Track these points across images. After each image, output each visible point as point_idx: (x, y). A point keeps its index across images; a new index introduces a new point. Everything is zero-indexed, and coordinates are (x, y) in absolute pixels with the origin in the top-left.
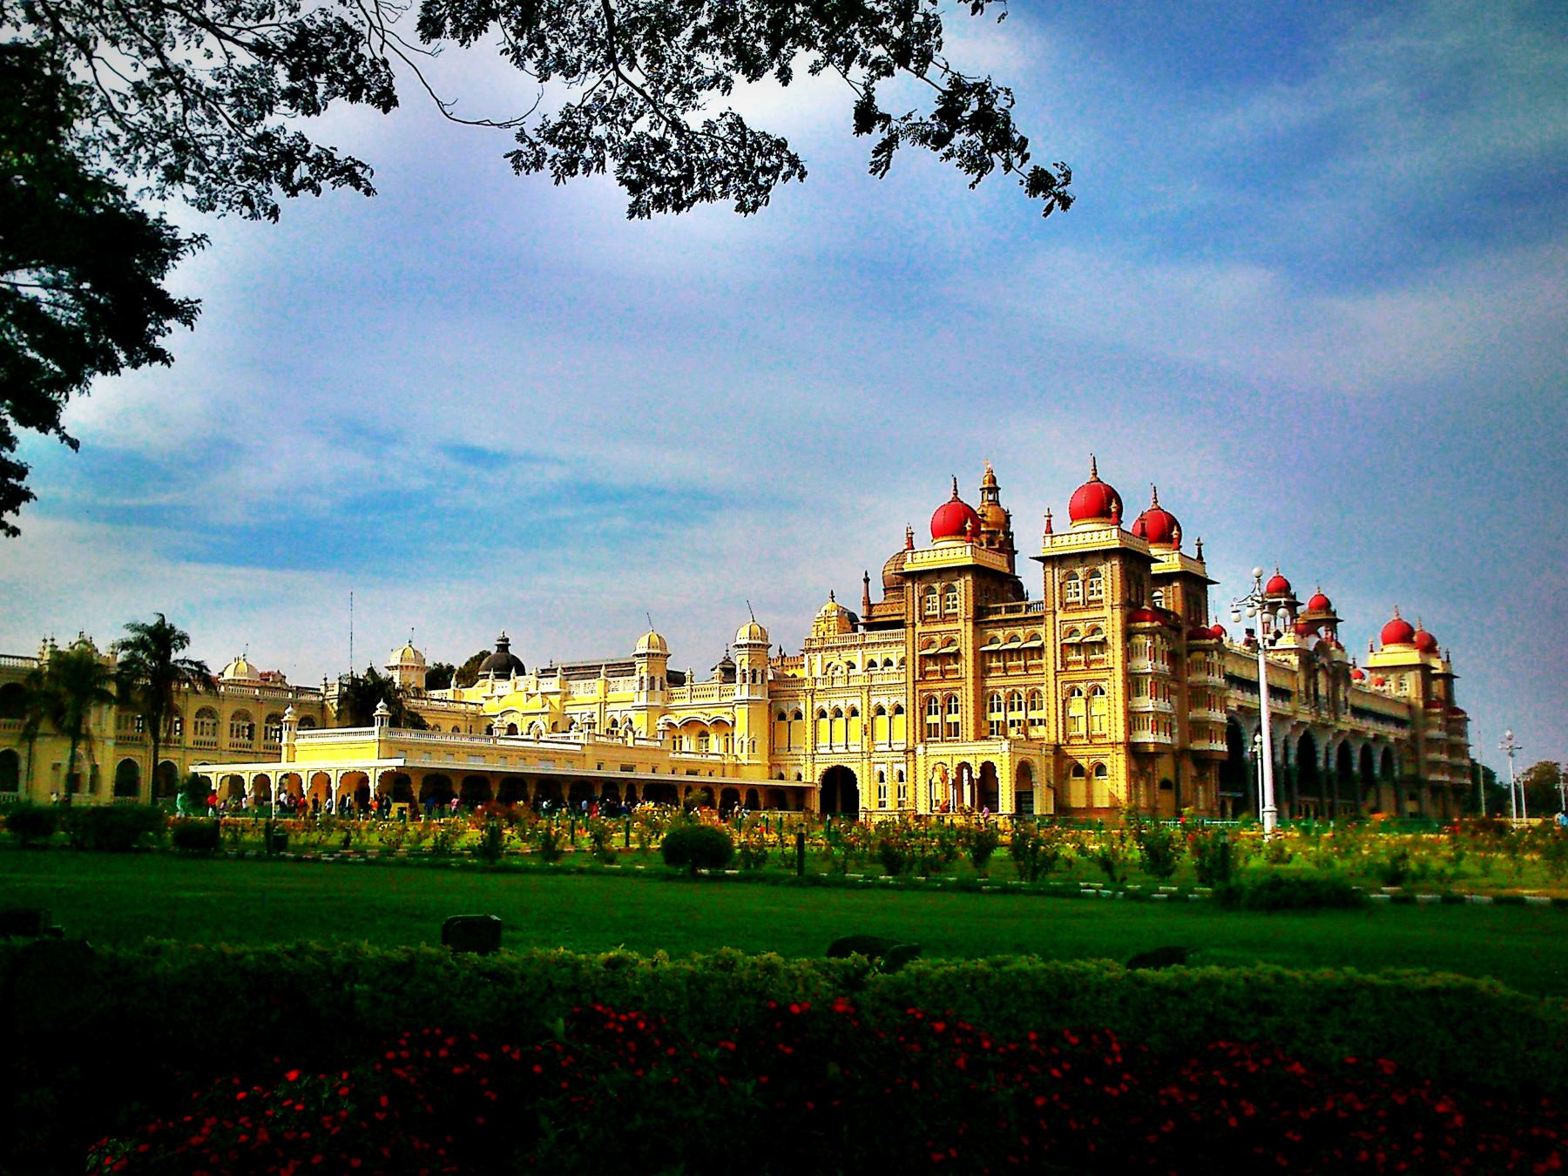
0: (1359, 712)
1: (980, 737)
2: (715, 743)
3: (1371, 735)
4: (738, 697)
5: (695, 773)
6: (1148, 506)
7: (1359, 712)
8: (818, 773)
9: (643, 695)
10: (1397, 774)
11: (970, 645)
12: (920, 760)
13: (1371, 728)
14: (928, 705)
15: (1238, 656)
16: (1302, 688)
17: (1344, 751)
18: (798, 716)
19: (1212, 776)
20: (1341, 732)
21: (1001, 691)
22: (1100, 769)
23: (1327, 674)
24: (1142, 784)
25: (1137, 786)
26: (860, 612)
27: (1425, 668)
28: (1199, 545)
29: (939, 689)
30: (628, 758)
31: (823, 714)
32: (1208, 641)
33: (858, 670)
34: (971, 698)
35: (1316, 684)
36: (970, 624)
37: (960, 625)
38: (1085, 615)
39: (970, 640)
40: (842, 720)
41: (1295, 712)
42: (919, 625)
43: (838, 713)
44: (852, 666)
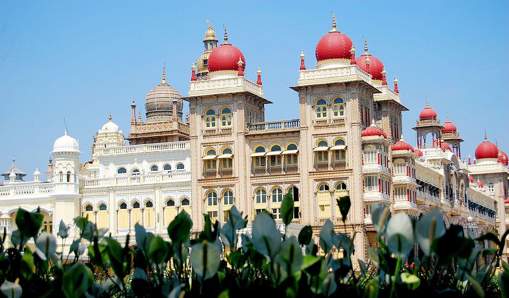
18: (103, 207)
29: (219, 186)
31: (123, 206)
34: (243, 193)
36: (242, 137)
43: (136, 205)
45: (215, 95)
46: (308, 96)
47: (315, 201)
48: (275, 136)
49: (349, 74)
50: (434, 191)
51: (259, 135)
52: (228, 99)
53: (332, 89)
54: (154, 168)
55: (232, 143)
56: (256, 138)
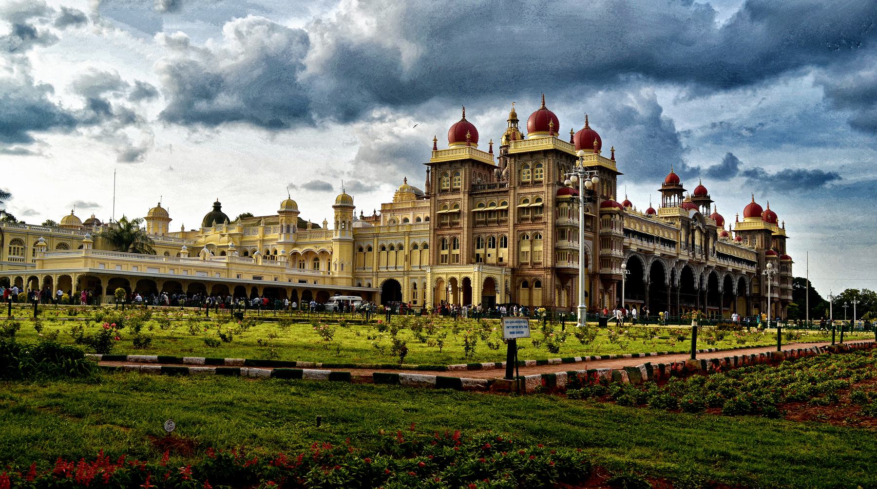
0: (721, 255)
1: (469, 262)
2: (323, 266)
3: (730, 269)
4: (334, 237)
5: (304, 282)
7: (721, 255)
8: (380, 283)
9: (283, 236)
10: (748, 293)
11: (466, 208)
13: (731, 265)
15: (638, 220)
16: (683, 239)
17: (713, 279)
18: (370, 249)
19: (613, 288)
20: (709, 267)
21: (483, 236)
22: (538, 284)
23: (701, 232)
25: (560, 294)
26: (424, 190)
27: (767, 232)
28: (613, 151)
29: (448, 234)
30: (257, 272)
31: (383, 249)
32: (613, 209)
33: (411, 222)
34: (466, 240)
36: (467, 195)
37: (461, 196)
38: (533, 190)
39: (466, 205)
40: (393, 252)
41: (678, 254)
43: (392, 248)
44: (406, 220)
47: (518, 249)
50: (671, 243)
52: (458, 165)
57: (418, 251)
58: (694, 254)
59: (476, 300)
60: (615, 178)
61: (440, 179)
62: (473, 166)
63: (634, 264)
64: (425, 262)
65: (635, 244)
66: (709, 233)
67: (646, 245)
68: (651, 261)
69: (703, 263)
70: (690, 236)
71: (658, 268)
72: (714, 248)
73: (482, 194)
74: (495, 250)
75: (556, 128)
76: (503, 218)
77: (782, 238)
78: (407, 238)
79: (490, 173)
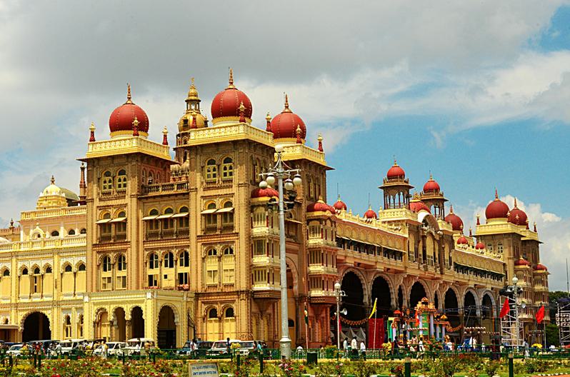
0: (459, 268)
3: (471, 284)
6: (275, 110)
7: (459, 268)
12: (86, 306)
13: (471, 280)
14: (105, 264)
16: (412, 249)
22: (230, 313)
23: (434, 239)
24: (262, 322)
25: (258, 323)
29: (112, 250)
31: (25, 272)
34: (134, 258)
35: (424, 247)
36: (135, 200)
37: (127, 200)
41: (406, 268)
42: (98, 200)
45: (109, 156)
46: (198, 156)
47: (202, 267)
48: (166, 198)
49: (237, 132)
50: (397, 255)
51: (151, 197)
52: (124, 160)
53: (222, 148)
54: (72, 232)
55: (126, 204)
56: (150, 200)
57: (69, 275)
58: (426, 268)
59: (150, 334)
60: (324, 174)
61: (99, 179)
62: (142, 160)
63: (351, 282)
64: (81, 289)
65: (352, 257)
66: (444, 241)
67: (365, 258)
68: (372, 278)
69: (438, 279)
70: (421, 244)
71: (381, 287)
72: (450, 258)
73: (154, 197)
74: (173, 269)
75: (248, 113)
76: (183, 228)
77: (536, 243)
78: (56, 257)
79: (165, 169)
